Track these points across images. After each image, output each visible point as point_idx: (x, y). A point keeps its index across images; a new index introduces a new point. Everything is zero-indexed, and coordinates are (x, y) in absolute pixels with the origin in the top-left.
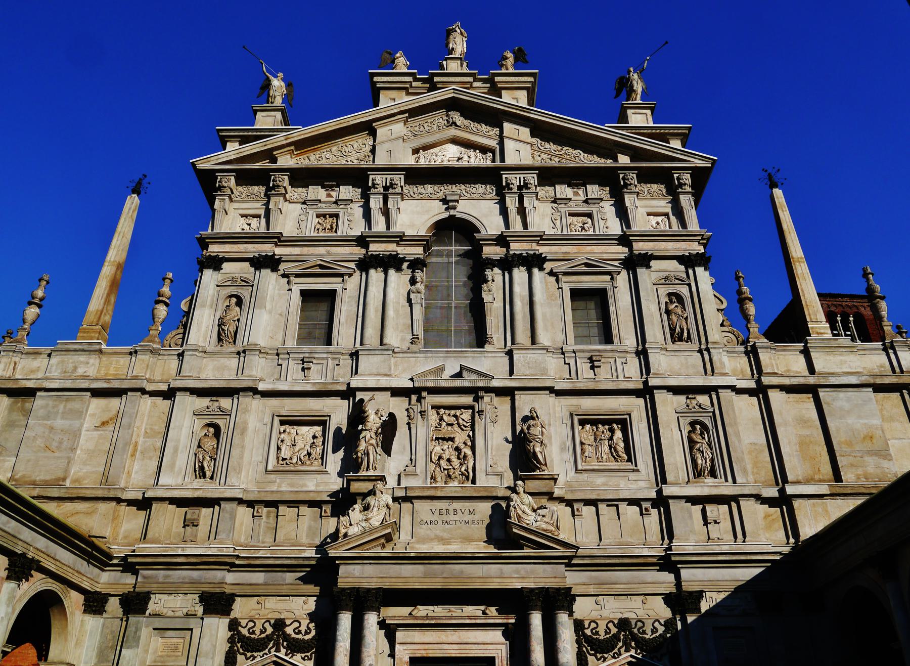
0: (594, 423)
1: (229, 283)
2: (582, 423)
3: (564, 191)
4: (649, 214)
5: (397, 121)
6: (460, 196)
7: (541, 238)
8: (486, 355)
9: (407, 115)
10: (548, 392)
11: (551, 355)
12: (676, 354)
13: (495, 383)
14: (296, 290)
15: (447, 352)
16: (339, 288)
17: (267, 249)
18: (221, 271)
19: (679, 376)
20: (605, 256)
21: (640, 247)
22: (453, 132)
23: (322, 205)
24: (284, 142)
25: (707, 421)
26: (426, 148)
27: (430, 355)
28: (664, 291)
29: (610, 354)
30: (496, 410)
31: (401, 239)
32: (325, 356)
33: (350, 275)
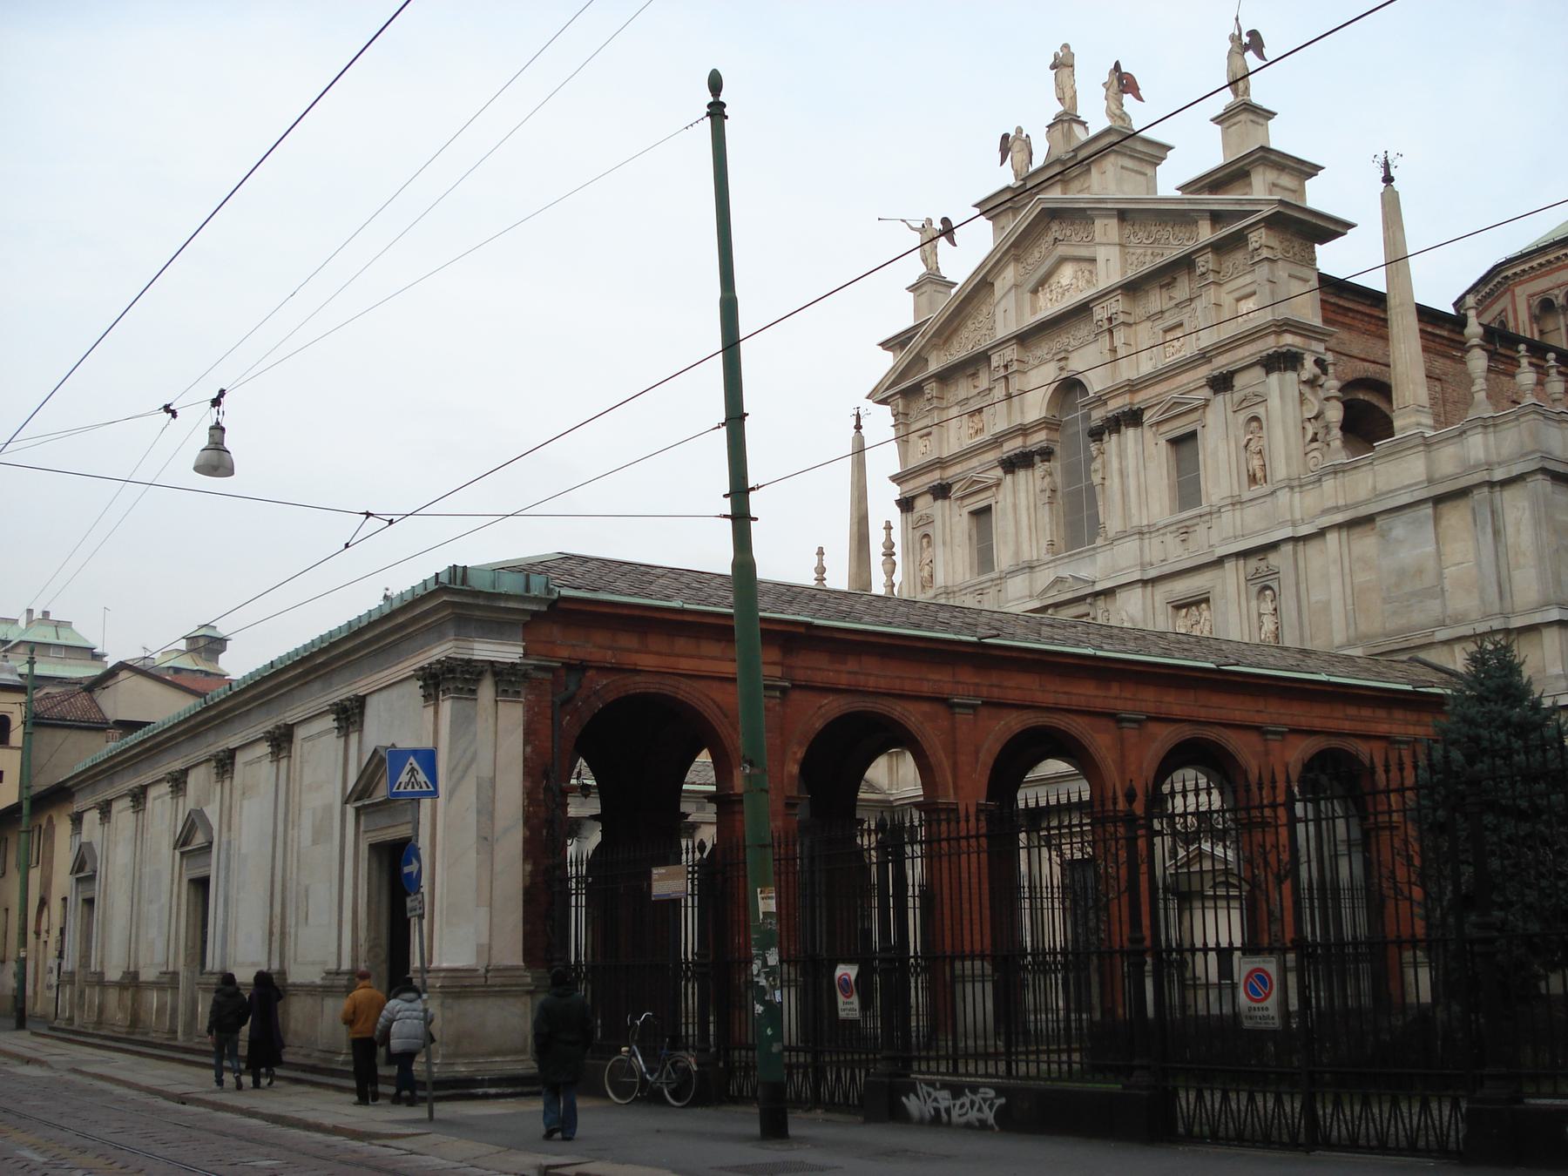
0: (1187, 605)
1: (920, 523)
2: (1178, 608)
3: (1155, 300)
4: (1238, 300)
5: (1007, 265)
6: (1066, 351)
7: (1133, 387)
8: (1098, 550)
9: (1013, 251)
10: (1140, 585)
11: (1148, 536)
12: (1254, 503)
13: (1098, 587)
14: (965, 512)
15: (1070, 556)
16: (993, 502)
17: (934, 477)
18: (915, 510)
19: (1255, 533)
20: (1192, 386)
21: (1222, 363)
22: (1062, 250)
23: (971, 401)
24: (923, 342)
25: (1275, 585)
26: (1043, 282)
27: (1058, 562)
28: (1243, 417)
29: (1194, 521)
30: (1106, 614)
31: (1023, 430)
32: (989, 584)
33: (998, 485)
